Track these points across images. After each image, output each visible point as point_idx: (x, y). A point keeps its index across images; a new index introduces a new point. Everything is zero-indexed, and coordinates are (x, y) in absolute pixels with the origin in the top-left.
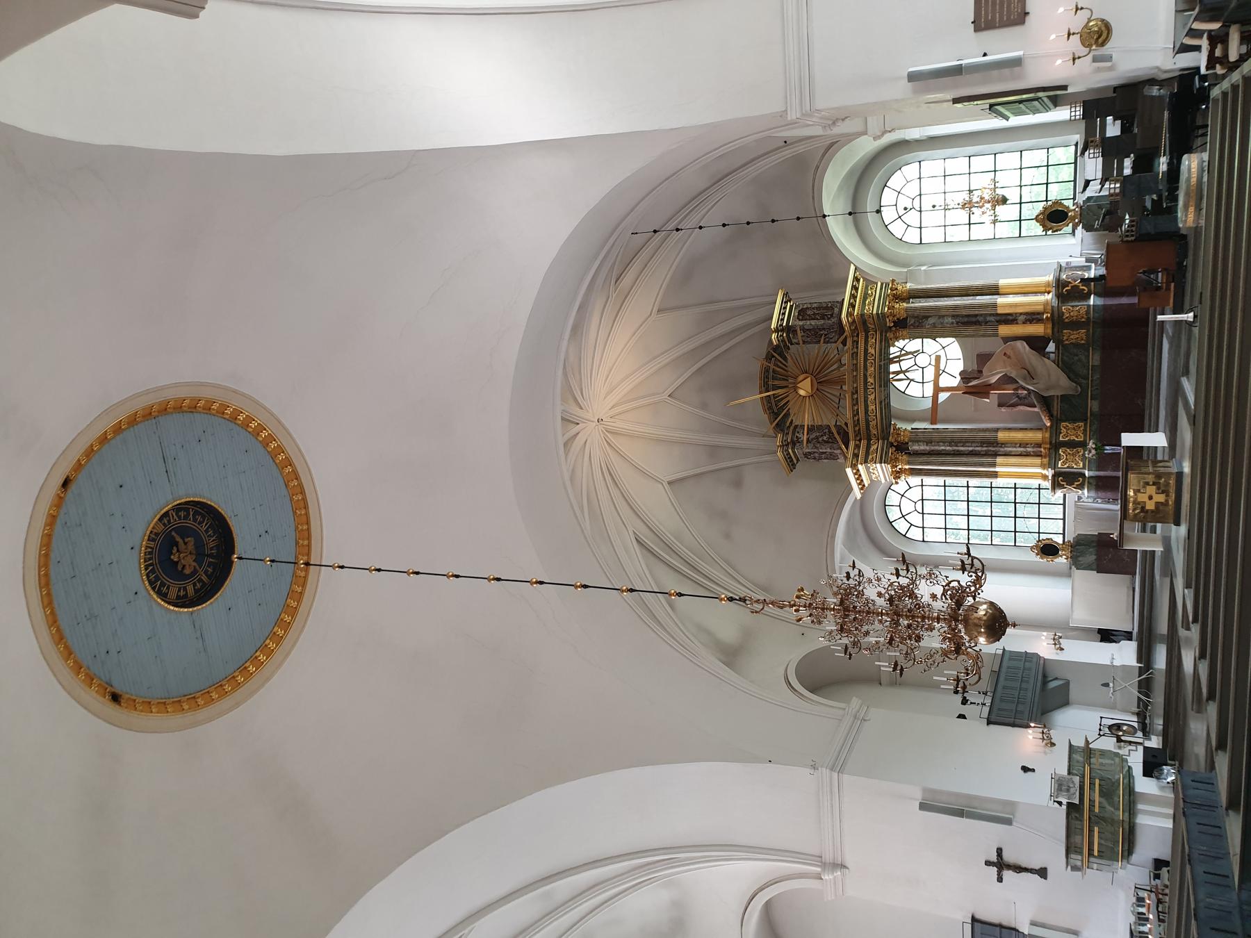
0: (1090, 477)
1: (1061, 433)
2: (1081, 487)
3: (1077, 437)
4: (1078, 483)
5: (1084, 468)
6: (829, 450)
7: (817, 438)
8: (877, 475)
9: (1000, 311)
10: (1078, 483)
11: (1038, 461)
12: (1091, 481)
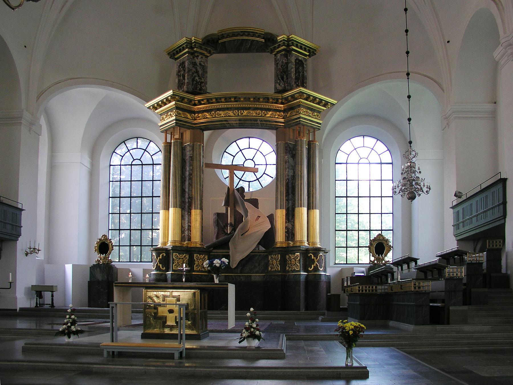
0: (166, 275)
1: (200, 255)
2: (158, 268)
3: (197, 266)
4: (161, 267)
5: (173, 270)
6: (186, 81)
7: (197, 72)
8: (166, 119)
9: (297, 209)
10: (161, 267)
11: (178, 238)
12: (163, 276)
